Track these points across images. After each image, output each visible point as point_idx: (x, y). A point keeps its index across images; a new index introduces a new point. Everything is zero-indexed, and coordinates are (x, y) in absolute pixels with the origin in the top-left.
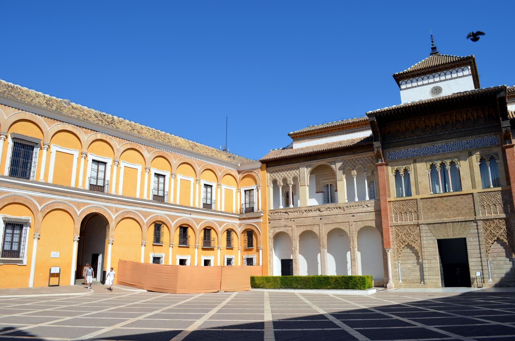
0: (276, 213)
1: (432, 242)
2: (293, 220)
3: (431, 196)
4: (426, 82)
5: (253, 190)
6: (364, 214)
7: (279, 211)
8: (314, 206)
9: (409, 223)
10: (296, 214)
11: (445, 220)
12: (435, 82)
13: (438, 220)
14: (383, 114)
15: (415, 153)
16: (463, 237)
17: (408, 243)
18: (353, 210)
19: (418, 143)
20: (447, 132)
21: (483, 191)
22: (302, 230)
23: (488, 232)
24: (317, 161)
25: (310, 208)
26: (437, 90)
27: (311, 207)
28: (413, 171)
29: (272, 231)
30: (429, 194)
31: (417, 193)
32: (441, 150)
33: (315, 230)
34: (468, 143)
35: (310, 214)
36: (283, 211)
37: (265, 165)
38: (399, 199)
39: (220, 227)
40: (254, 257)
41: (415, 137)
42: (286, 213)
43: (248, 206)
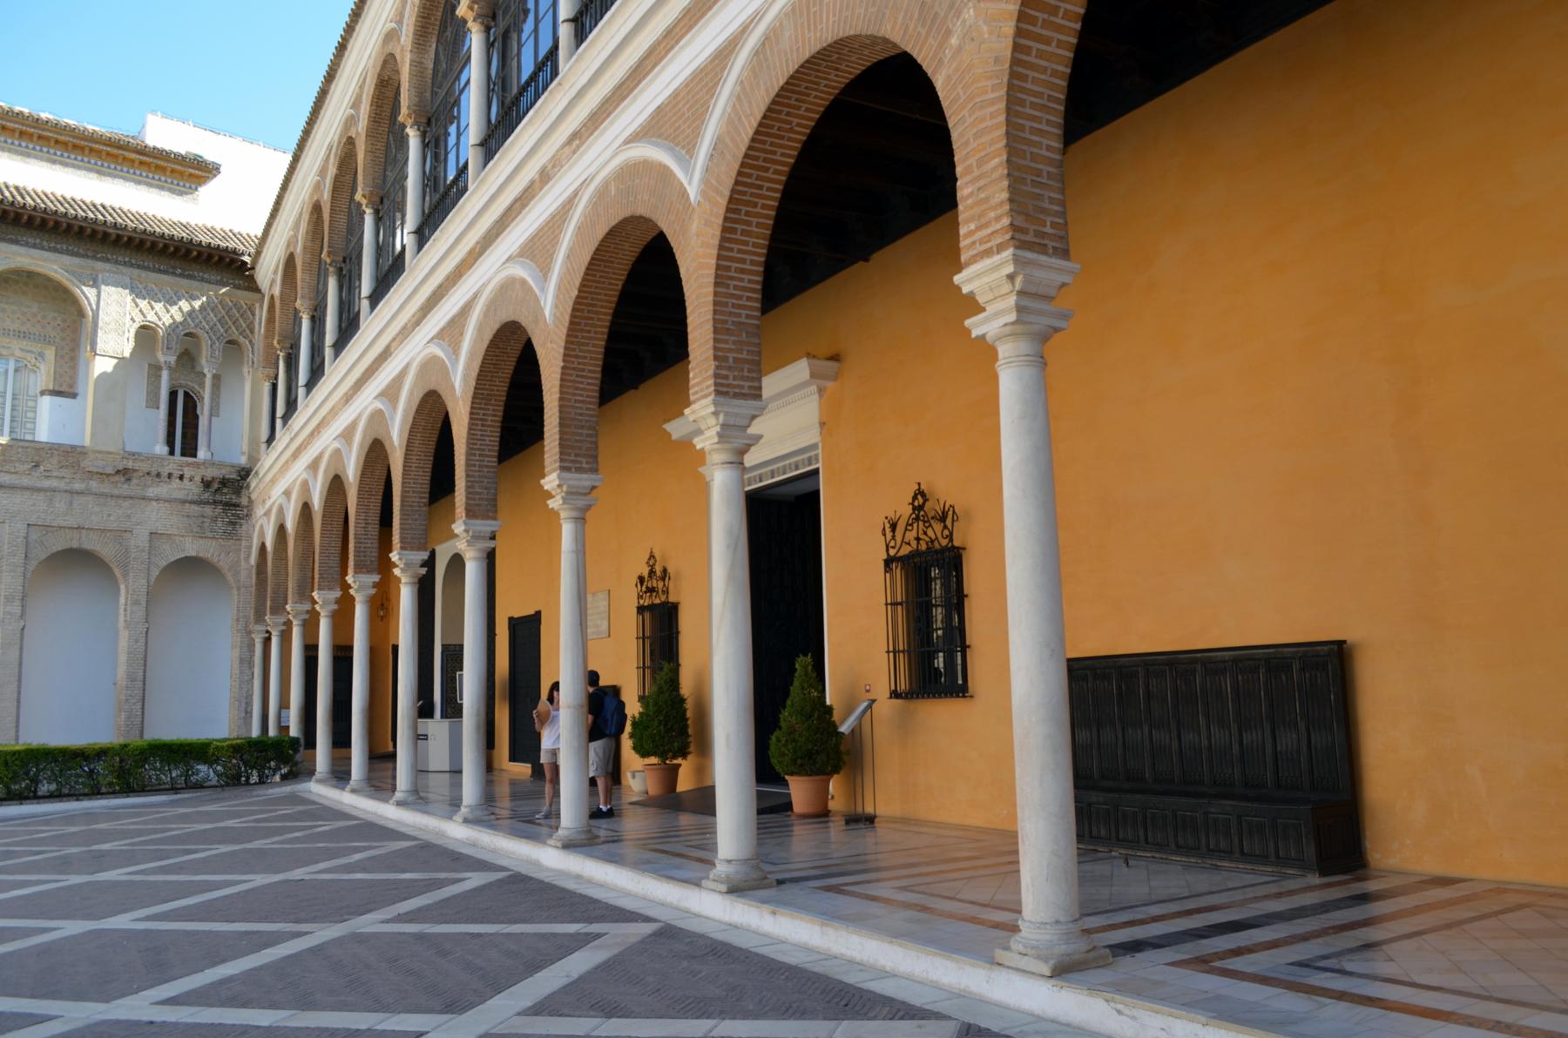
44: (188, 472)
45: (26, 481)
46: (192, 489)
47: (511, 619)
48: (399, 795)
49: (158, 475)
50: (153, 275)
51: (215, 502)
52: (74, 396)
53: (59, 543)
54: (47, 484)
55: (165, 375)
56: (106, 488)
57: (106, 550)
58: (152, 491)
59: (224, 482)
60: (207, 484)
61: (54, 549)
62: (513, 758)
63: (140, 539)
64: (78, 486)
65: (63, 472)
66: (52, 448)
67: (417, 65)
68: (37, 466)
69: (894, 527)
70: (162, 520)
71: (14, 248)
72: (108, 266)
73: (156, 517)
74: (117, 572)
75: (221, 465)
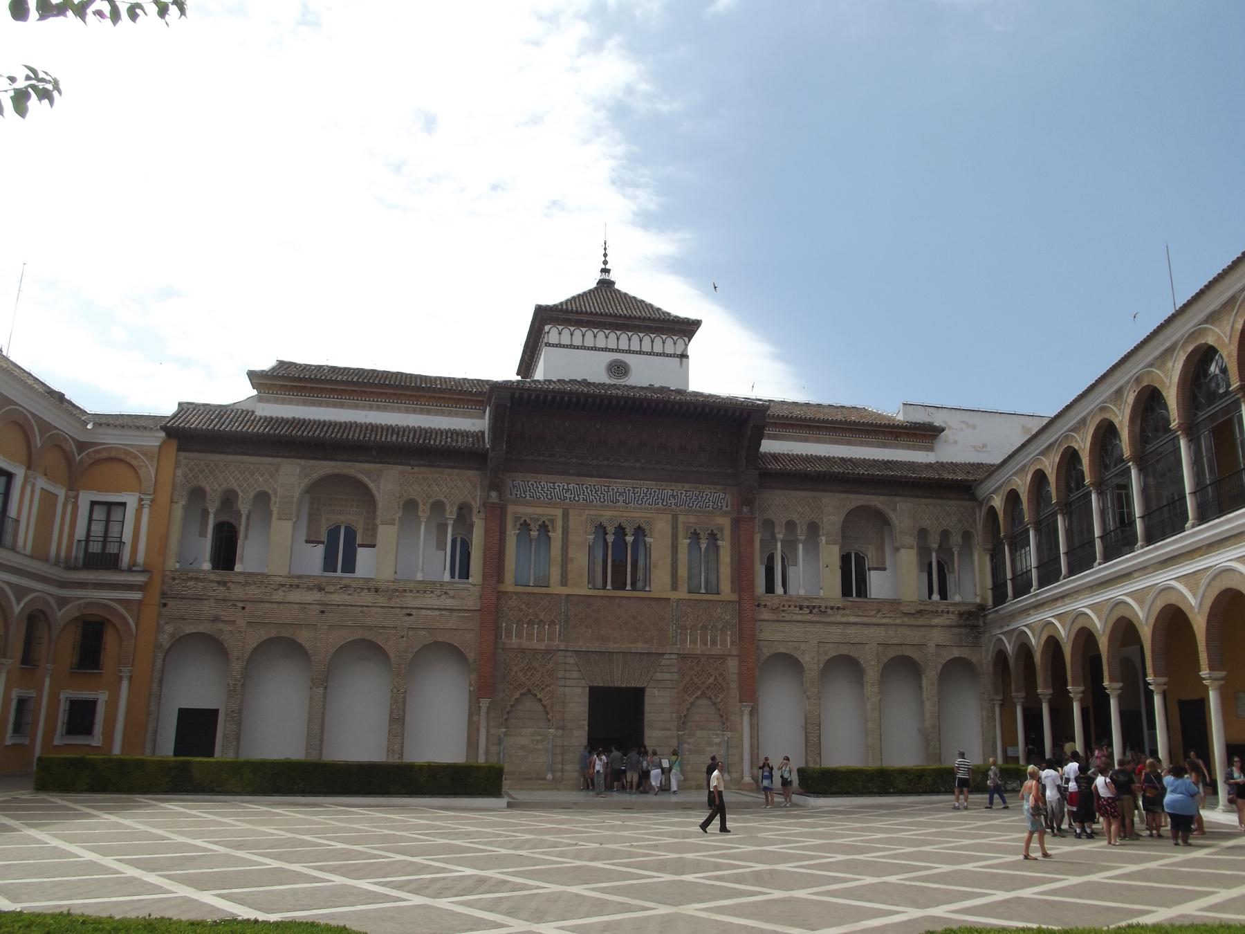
0: (191, 578)
1: (578, 691)
2: (240, 604)
3: (589, 592)
4: (601, 341)
5: (124, 504)
6: (437, 613)
7: (201, 575)
8: (309, 577)
9: (535, 644)
10: (253, 592)
11: (612, 647)
12: (618, 350)
13: (596, 646)
14: (530, 395)
15: (568, 495)
16: (639, 685)
17: (529, 690)
18: (410, 601)
19: (579, 475)
20: (638, 465)
21: (688, 596)
22: (264, 634)
23: (688, 679)
24: (333, 463)
25: (296, 581)
26: (619, 369)
27: (300, 577)
28: (559, 531)
29: (169, 628)
30: (583, 590)
31: (564, 582)
32: (621, 499)
33: (304, 637)
34: (673, 496)
35: (295, 596)
36: (213, 577)
37: (174, 445)
38: (520, 589)
39: (19, 601)
40: (102, 697)
41: (574, 460)
42: (224, 583)
43: (95, 548)
45: (874, 621)
51: (966, 626)
52: (885, 569)
53: (893, 653)
54: (884, 621)
55: (934, 555)
57: (915, 655)
58: (935, 621)
59: (970, 613)
60: (961, 615)
63: (932, 649)
64: (898, 621)
65: (891, 614)
66: (885, 601)
73: (937, 636)
75: (969, 604)
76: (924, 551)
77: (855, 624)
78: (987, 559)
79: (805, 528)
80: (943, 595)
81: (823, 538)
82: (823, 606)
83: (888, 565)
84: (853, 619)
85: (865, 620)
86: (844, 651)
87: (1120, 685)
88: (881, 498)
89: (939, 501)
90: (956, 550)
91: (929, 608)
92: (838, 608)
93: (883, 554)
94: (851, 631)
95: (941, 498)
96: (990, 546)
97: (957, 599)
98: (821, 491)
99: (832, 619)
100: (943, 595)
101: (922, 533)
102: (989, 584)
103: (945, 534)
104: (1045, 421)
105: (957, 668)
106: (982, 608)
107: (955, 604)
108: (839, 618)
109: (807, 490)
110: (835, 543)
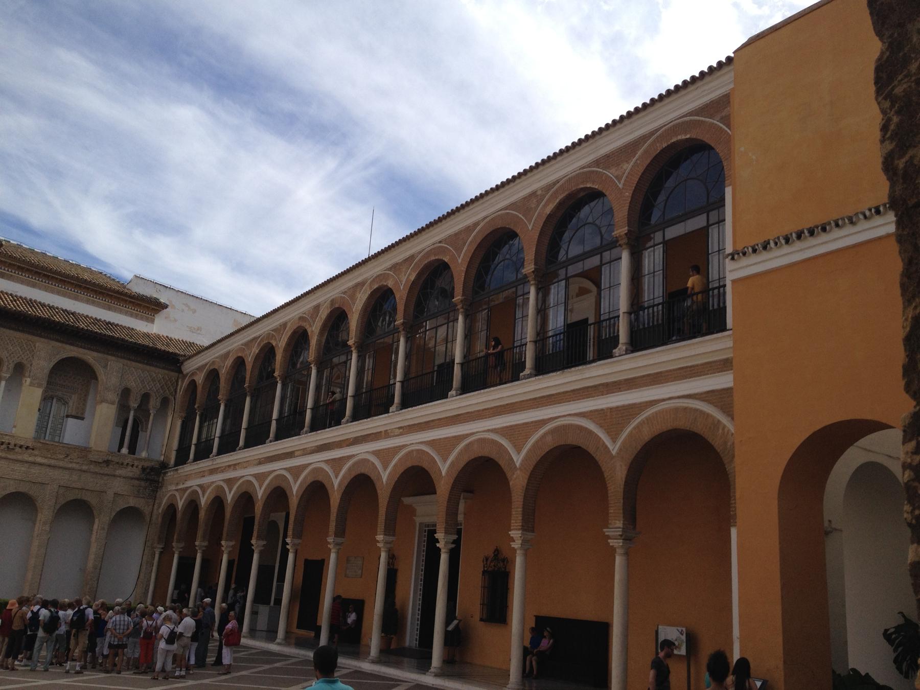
44: (136, 463)
45: (61, 464)
46: (136, 472)
47: (306, 560)
48: (278, 641)
49: (122, 464)
50: (134, 364)
51: (147, 480)
52: (82, 419)
54: (70, 465)
56: (97, 469)
57: (93, 501)
58: (118, 472)
60: (144, 469)
61: (69, 499)
62: (298, 627)
64: (84, 467)
67: (319, 341)
68: (67, 456)
69: (487, 560)
70: (119, 489)
71: (72, 347)
72: (113, 358)
74: (95, 513)
75: (152, 460)
76: (123, 407)
77: (41, 464)
78: (179, 423)
79: (12, 366)
80: (132, 449)
81: (28, 380)
82: (13, 443)
83: (86, 415)
84: (39, 460)
85: (53, 462)
86: (23, 489)
87: (265, 543)
88: (95, 354)
89: (148, 367)
90: (152, 412)
91: (116, 459)
92: (27, 448)
93: (84, 405)
94: (35, 470)
95: (150, 365)
96: (184, 415)
97: (144, 455)
98: (37, 335)
99: (20, 457)
100: (132, 449)
101: (126, 393)
102: (175, 444)
103: (146, 397)
104: (252, 320)
105: (128, 516)
106: (164, 466)
107: (140, 460)
108: (26, 457)
109: (22, 331)
110: (39, 386)
